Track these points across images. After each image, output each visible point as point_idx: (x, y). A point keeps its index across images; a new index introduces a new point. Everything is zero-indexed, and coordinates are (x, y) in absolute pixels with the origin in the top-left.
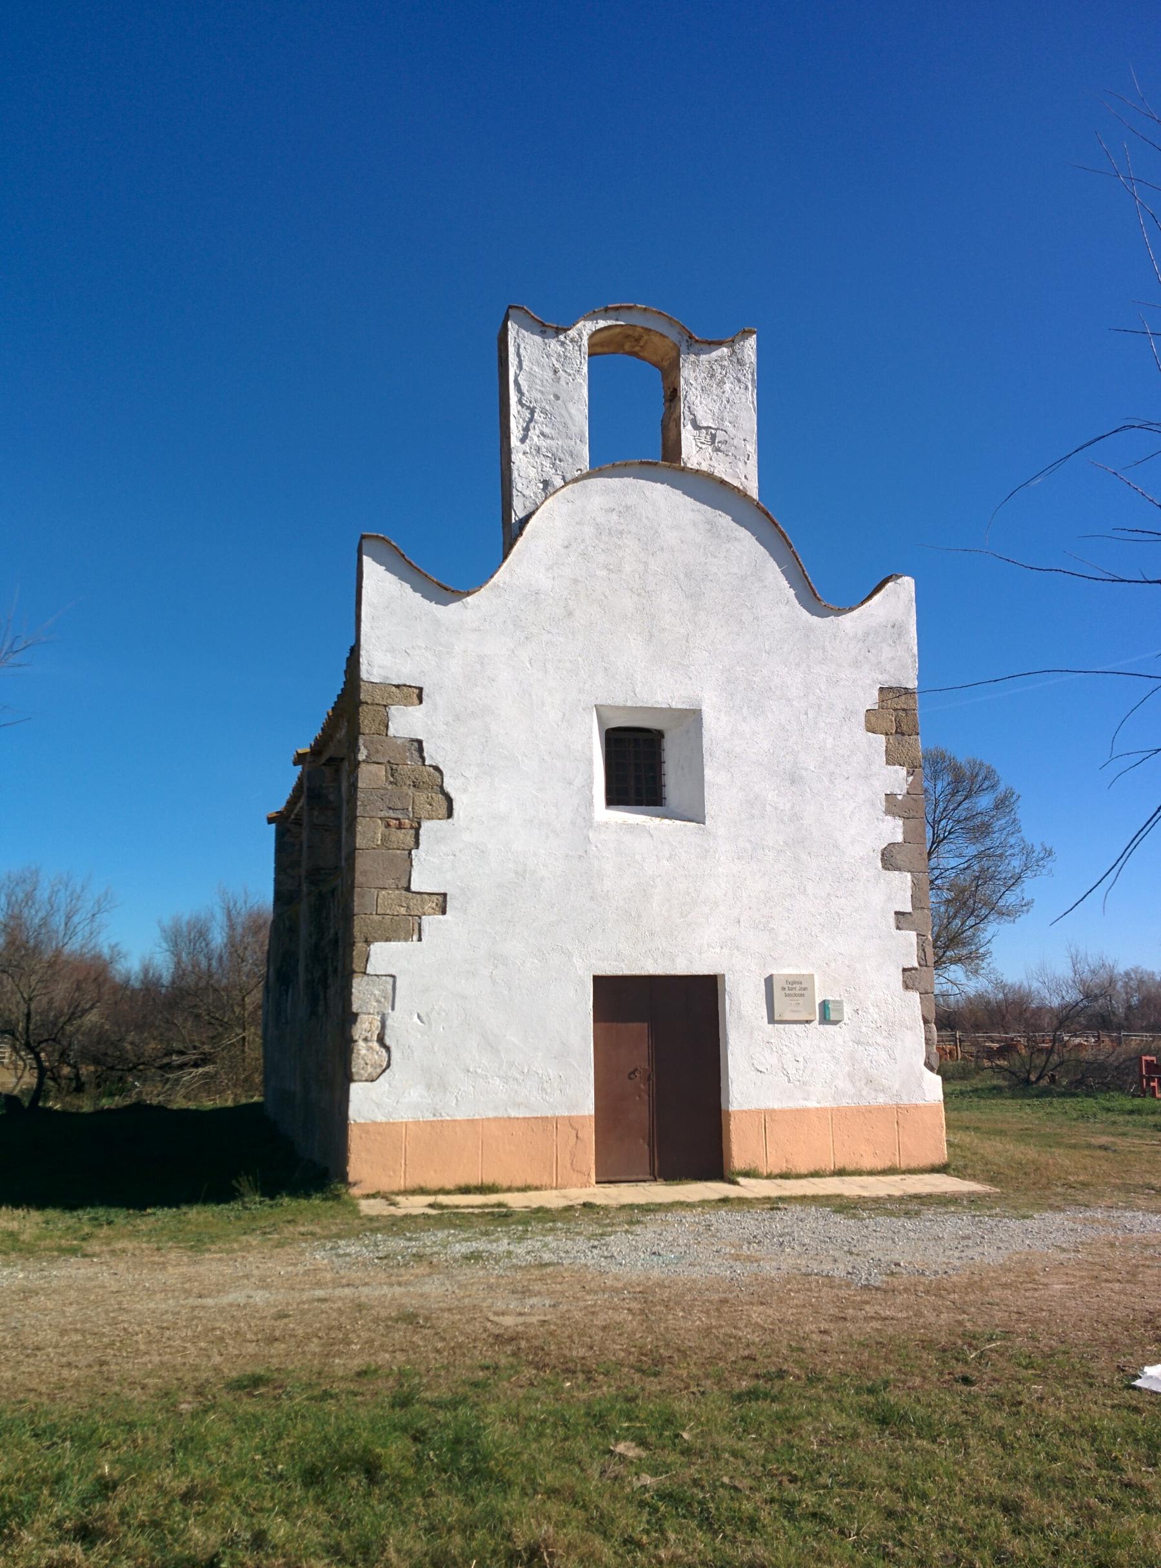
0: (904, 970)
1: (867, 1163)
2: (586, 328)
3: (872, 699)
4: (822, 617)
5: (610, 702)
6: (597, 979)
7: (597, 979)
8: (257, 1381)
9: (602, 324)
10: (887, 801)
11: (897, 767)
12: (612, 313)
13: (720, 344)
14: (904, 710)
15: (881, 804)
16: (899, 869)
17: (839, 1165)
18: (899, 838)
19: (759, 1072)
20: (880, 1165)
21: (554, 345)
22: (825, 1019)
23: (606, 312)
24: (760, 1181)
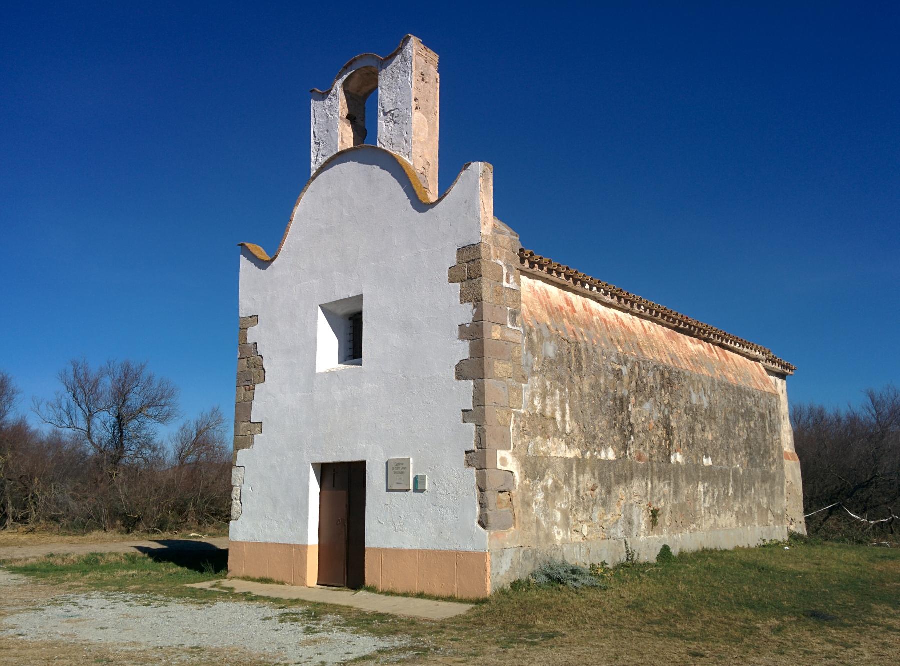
0: (467, 452)
1: (438, 591)
2: (339, 84)
3: (452, 259)
4: (424, 212)
5: (333, 300)
6: (364, 463)
7: (364, 463)
8: (815, 615)
9: (345, 77)
10: (460, 329)
11: (467, 304)
12: (349, 68)
13: (395, 55)
14: (473, 261)
15: (457, 333)
16: (466, 379)
17: (421, 590)
18: (467, 356)
19: (387, 525)
20: (445, 594)
21: (327, 102)
22: (416, 490)
23: (346, 69)
24: (310, 600)
